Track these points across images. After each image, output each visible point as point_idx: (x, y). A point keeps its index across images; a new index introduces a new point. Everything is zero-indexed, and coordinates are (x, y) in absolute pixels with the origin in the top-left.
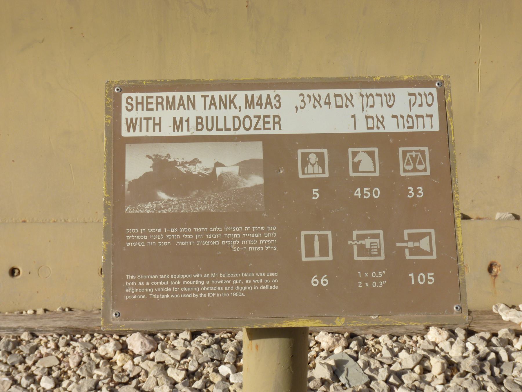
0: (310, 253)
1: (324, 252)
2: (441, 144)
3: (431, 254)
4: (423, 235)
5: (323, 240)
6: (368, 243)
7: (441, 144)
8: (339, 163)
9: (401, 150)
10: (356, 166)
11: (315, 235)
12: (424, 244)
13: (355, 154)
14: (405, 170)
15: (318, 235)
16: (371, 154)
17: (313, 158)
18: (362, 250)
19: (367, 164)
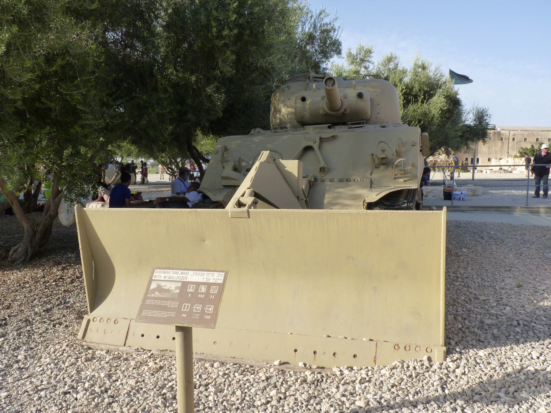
2: (222, 287)
5: (188, 306)
6: (197, 308)
7: (222, 287)
12: (210, 309)
14: (211, 291)
17: (192, 287)
18: (196, 309)
19: (203, 289)
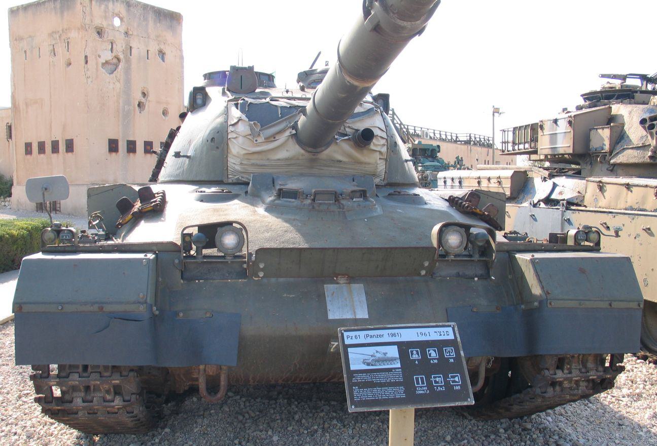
0: (418, 383)
1: (423, 383)
3: (459, 382)
4: (456, 376)
6: (437, 379)
8: (424, 354)
9: (444, 349)
10: (430, 355)
11: (418, 378)
12: (456, 379)
13: (429, 351)
14: (446, 355)
15: (421, 377)
16: (435, 351)
18: (436, 382)
19: (433, 353)
